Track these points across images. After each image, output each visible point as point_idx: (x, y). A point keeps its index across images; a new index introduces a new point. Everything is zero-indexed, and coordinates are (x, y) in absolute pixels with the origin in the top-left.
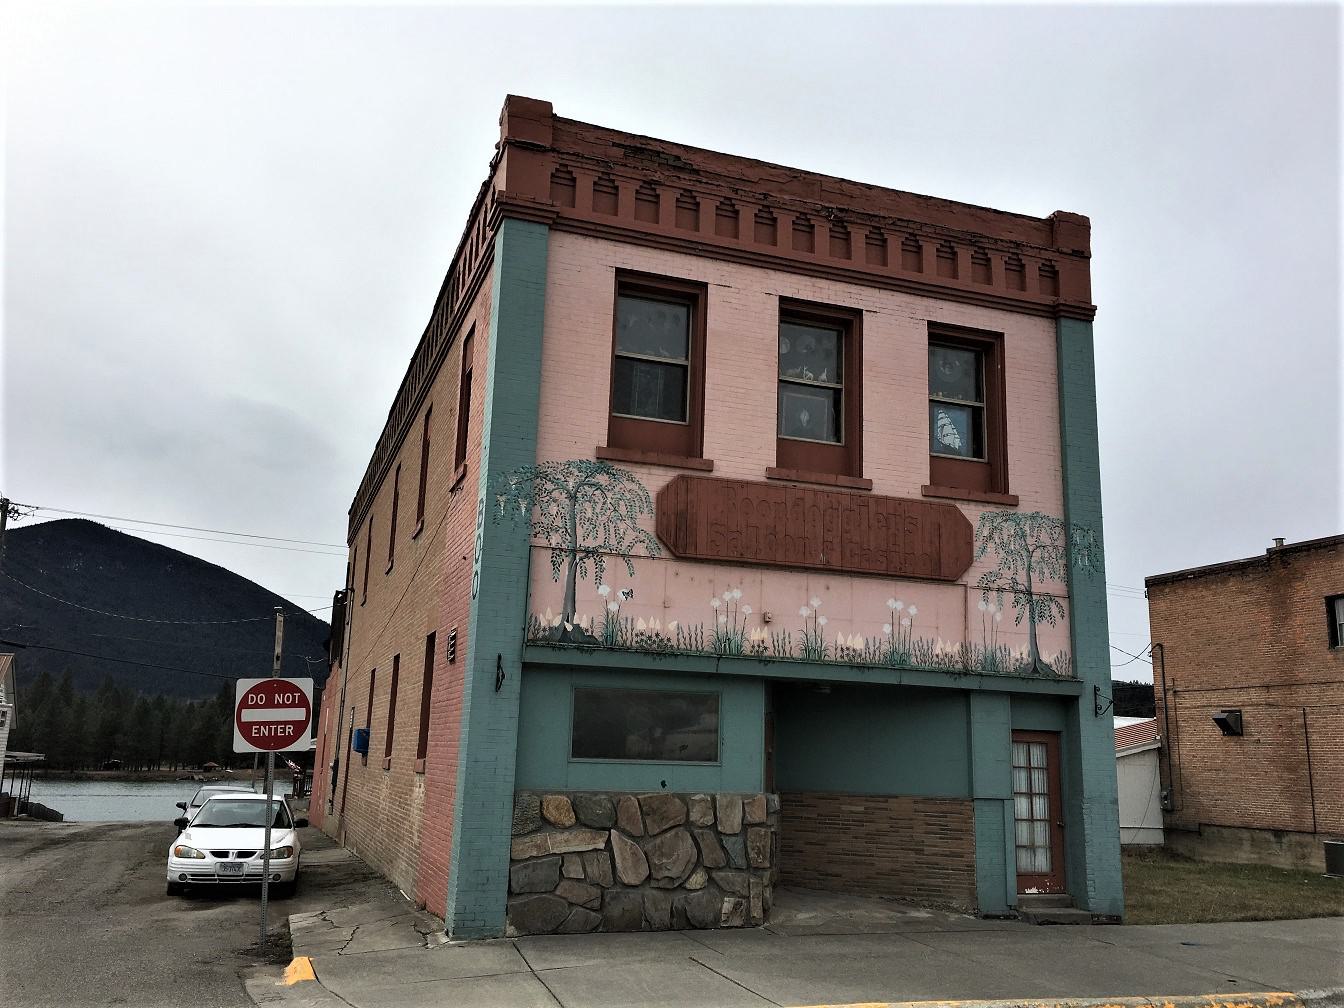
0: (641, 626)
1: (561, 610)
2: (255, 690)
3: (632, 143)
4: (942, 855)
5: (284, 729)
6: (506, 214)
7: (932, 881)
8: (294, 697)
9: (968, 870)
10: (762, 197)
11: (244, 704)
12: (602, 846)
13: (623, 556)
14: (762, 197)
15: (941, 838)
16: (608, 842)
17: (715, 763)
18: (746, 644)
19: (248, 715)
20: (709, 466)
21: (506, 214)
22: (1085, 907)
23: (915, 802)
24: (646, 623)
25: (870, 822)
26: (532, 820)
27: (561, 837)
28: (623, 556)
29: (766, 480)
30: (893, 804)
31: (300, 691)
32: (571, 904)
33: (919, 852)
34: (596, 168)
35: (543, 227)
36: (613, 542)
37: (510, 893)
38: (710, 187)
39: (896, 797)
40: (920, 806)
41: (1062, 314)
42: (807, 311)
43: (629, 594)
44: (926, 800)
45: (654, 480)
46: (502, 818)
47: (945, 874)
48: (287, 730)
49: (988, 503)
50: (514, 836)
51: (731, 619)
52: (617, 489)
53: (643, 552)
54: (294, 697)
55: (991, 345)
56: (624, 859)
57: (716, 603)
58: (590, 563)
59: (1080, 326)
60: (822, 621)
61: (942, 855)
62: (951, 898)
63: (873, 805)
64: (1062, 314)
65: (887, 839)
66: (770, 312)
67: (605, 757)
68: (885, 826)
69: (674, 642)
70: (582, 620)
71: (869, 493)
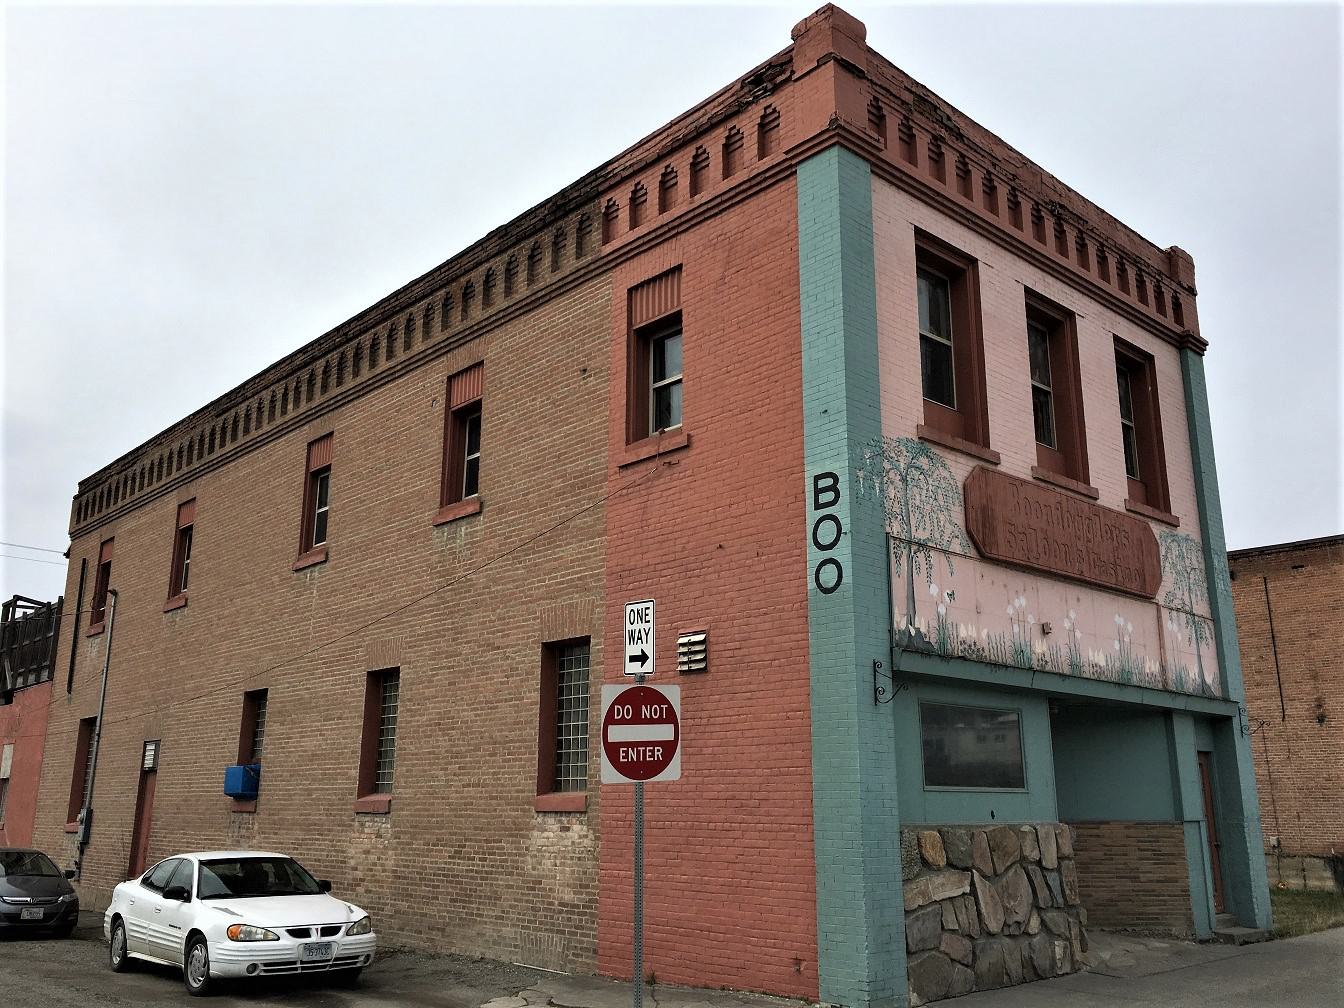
0: (963, 633)
1: (905, 612)
2: (621, 700)
3: (920, 92)
4: (1158, 881)
5: (653, 751)
6: (842, 141)
7: (1149, 909)
8: (661, 709)
9: (1183, 896)
10: (1011, 177)
11: (610, 720)
12: (967, 889)
13: (945, 551)
14: (1011, 177)
15: (1155, 864)
16: (972, 884)
17: (1023, 790)
18: (1034, 656)
19: (617, 733)
20: (1093, 497)
21: (842, 141)
22: (1252, 924)
23: (1127, 827)
24: (968, 632)
25: (1081, 850)
26: (919, 864)
27: (939, 880)
28: (945, 551)
29: (1124, 511)
30: (1104, 830)
31: (668, 703)
32: (952, 960)
33: (1135, 879)
34: (899, 109)
35: (866, 163)
36: (937, 536)
37: (909, 953)
38: (978, 156)
39: (1107, 823)
40: (1132, 832)
41: (1190, 345)
42: (936, 253)
43: (951, 595)
44: (1139, 824)
45: (959, 468)
46: (894, 867)
47: (1161, 900)
48: (656, 753)
49: (1162, 522)
50: (906, 881)
51: (1022, 628)
52: (935, 476)
53: (958, 550)
54: (661, 709)
55: (1059, 324)
56: (986, 904)
57: (1010, 611)
58: (921, 555)
59: (1196, 357)
60: (1078, 634)
61: (1158, 881)
62: (1170, 925)
63: (1085, 832)
64: (1190, 345)
65: (1101, 868)
66: (1019, 300)
67: (946, 784)
68: (1100, 854)
69: (987, 653)
70: (921, 623)
71: (994, 467)
